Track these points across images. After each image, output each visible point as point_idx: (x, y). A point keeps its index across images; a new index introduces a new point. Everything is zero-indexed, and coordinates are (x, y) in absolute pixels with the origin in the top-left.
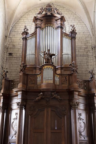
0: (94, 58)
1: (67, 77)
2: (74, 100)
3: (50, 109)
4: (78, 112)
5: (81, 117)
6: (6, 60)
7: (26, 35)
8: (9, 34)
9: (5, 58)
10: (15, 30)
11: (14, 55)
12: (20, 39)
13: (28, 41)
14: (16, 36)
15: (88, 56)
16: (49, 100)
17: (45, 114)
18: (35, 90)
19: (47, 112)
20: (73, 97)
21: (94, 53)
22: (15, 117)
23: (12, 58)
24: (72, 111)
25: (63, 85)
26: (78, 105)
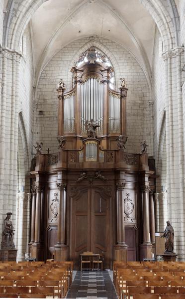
0: (151, 118)
1: (113, 154)
2: (120, 181)
3: (93, 191)
4: (124, 193)
5: (129, 198)
6: (36, 120)
7: (63, 91)
8: (37, 84)
9: (35, 119)
10: (46, 78)
11: (45, 113)
12: (53, 91)
13: (66, 101)
14: (47, 86)
15: (143, 115)
16: (93, 180)
17: (89, 196)
18: (77, 169)
19: (91, 193)
20: (120, 177)
21: (151, 111)
22: (54, 198)
23: (44, 118)
24: (118, 193)
25: (109, 163)
26: (124, 185)
